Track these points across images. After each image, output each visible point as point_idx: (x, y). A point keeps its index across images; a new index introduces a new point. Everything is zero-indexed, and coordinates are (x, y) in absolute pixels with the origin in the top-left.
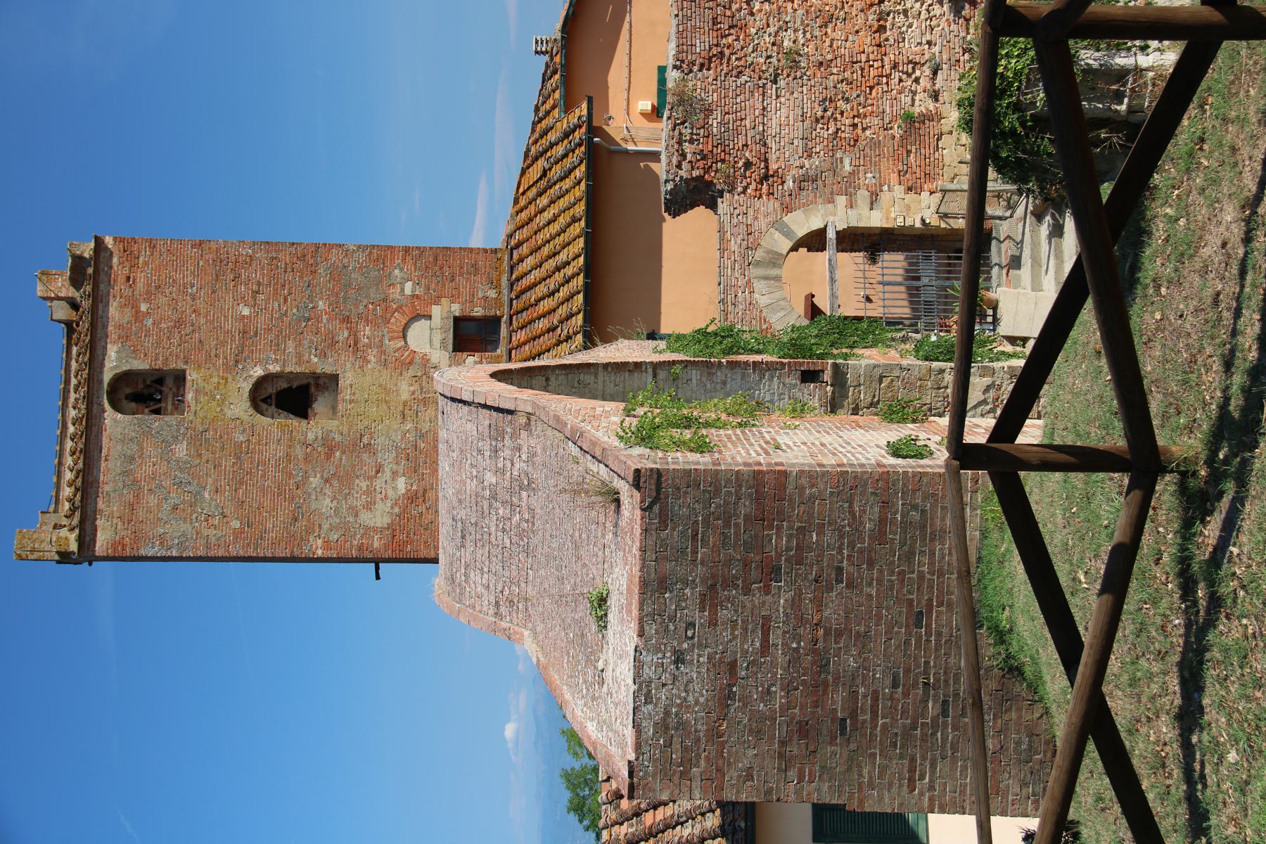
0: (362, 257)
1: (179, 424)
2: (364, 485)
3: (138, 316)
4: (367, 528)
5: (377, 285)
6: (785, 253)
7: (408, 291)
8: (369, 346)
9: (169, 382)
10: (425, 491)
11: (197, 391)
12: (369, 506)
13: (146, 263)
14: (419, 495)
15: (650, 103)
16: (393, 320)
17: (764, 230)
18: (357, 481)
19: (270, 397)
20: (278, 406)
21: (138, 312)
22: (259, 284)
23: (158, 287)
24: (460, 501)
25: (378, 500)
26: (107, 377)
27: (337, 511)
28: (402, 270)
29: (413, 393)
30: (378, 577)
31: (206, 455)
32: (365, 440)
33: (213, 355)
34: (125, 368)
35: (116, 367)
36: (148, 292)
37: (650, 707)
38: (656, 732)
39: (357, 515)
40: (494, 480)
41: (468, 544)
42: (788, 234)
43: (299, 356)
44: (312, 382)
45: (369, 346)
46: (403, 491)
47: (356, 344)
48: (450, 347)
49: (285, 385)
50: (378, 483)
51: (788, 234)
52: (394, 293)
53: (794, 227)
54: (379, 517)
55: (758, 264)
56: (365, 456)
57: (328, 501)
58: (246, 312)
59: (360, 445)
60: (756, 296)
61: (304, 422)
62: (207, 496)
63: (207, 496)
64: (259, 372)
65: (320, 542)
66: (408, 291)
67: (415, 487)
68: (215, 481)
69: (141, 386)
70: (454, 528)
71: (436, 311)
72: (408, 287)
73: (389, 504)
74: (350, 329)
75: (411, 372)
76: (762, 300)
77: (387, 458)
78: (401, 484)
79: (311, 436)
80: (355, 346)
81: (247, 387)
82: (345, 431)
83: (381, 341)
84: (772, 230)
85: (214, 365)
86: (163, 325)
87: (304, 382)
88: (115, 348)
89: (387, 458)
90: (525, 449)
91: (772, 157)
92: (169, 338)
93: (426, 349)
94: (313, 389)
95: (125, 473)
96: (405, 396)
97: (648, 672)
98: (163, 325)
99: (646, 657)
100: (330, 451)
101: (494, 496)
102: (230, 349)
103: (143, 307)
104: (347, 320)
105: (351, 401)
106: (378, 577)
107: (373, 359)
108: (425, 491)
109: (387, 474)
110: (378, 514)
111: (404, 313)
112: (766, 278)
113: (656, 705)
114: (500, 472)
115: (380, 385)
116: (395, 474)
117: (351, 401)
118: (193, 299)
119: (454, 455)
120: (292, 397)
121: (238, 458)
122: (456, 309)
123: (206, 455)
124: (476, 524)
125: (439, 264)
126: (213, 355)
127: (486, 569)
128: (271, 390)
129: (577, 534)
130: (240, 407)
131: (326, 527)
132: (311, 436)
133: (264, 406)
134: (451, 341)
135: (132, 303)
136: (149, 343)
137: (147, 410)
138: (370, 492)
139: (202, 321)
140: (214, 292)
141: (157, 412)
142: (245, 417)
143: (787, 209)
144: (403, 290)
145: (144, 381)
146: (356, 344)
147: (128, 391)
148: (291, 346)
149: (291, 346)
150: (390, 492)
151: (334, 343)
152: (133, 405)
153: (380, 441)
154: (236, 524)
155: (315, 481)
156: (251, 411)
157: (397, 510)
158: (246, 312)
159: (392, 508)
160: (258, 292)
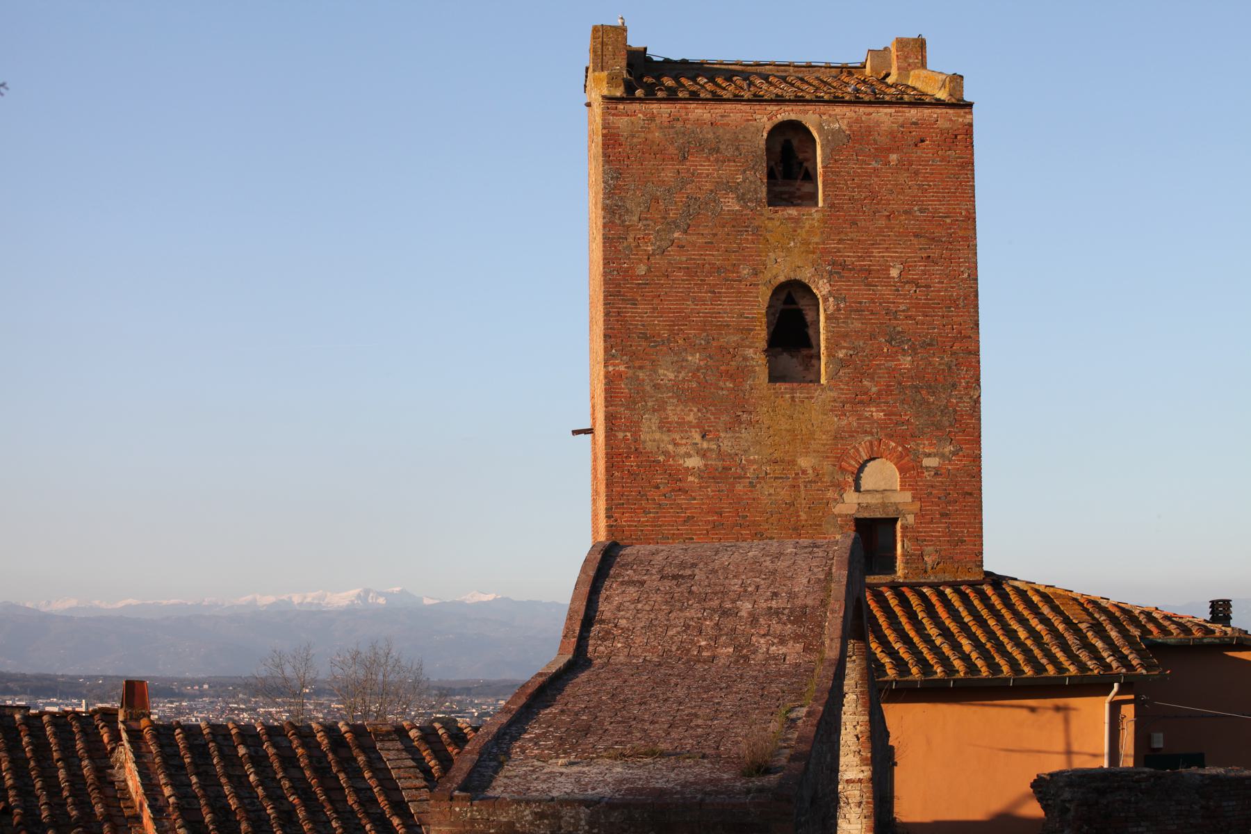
0: (965, 406)
1: (759, 202)
2: (691, 418)
5: (933, 424)
7: (927, 462)
9: (807, 188)
11: (796, 221)
12: (665, 426)
15: (1161, 746)
19: (794, 302)
20: (782, 311)
21: (890, 150)
24: (714, 571)
26: (810, 118)
27: (657, 387)
28: (955, 453)
30: (576, 432)
37: (529, 818)
38: (500, 824)
40: (743, 613)
41: (667, 583)
44: (814, 351)
47: (861, 402)
48: (861, 516)
49: (809, 318)
54: (651, 435)
56: (724, 418)
57: (672, 376)
58: (894, 273)
59: (738, 412)
61: (763, 345)
62: (676, 235)
63: (676, 235)
64: (821, 288)
65: (622, 368)
66: (927, 462)
68: (694, 244)
69: (801, 156)
70: (682, 565)
71: (907, 497)
73: (670, 448)
74: (879, 393)
75: (827, 466)
78: (694, 462)
80: (860, 400)
81: (805, 275)
82: (756, 393)
83: (866, 432)
85: (828, 238)
87: (814, 343)
88: (844, 127)
89: (726, 445)
90: (783, 650)
94: (805, 352)
95: (701, 145)
96: (803, 462)
97: (567, 813)
99: (584, 812)
100: (731, 377)
101: (725, 613)
102: (850, 257)
103: (894, 157)
104: (888, 390)
105: (793, 398)
106: (576, 432)
109: (705, 445)
110: (657, 436)
113: (532, 823)
114: (754, 619)
115: (813, 433)
116: (703, 454)
117: (793, 398)
118: (906, 212)
119: (768, 563)
120: (790, 327)
124: (690, 592)
125: (960, 497)
127: (640, 606)
128: (803, 303)
129: (700, 722)
130: (781, 271)
131: (641, 375)
132: (750, 352)
133: (783, 296)
134: (866, 515)
135: (896, 141)
137: (773, 163)
139: (882, 223)
140: (916, 236)
141: (771, 175)
144: (929, 455)
145: (807, 160)
146: (861, 402)
147: (795, 143)
149: (857, 325)
150: (682, 450)
152: (778, 148)
153: (746, 435)
155: (695, 359)
156: (776, 282)
157: (661, 458)
158: (894, 273)
159: (666, 453)
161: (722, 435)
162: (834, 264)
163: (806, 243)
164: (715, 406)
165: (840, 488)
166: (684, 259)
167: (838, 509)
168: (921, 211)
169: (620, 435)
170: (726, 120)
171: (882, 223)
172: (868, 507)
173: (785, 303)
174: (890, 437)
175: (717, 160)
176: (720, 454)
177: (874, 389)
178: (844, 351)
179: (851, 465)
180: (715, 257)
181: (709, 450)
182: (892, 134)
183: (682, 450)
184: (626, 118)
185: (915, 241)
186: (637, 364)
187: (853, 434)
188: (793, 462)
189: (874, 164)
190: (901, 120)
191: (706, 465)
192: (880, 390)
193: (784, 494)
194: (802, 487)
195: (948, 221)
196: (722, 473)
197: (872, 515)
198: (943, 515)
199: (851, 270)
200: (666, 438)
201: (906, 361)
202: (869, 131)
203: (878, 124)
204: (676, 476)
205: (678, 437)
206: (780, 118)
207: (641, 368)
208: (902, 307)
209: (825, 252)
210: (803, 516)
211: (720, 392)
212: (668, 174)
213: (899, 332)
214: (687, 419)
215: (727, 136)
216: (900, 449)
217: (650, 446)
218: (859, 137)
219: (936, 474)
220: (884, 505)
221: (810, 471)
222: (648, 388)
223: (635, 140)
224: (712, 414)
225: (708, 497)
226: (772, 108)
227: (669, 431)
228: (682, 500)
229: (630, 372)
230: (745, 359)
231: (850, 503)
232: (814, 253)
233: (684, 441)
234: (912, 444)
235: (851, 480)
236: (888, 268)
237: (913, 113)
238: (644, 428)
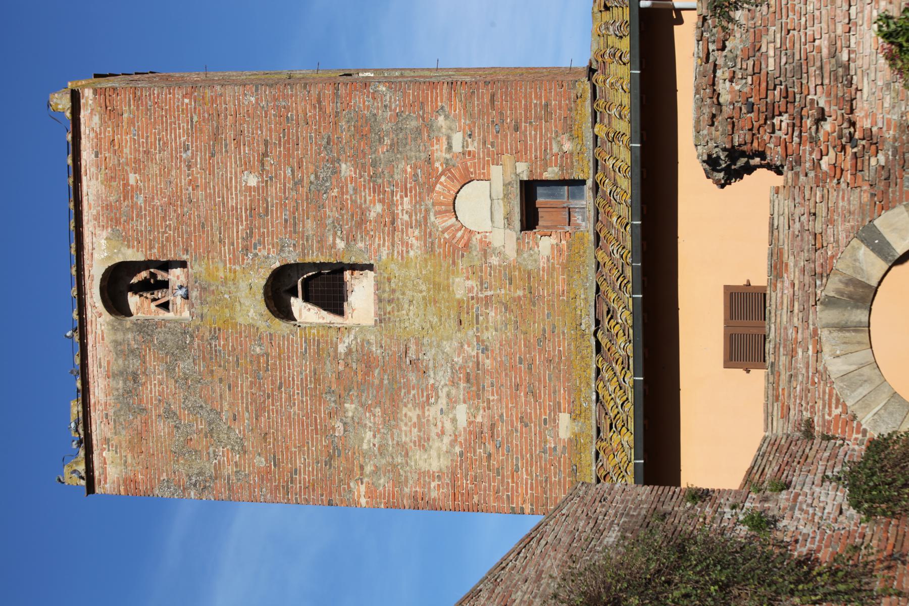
3: (127, 192)
4: (422, 474)
5: (415, 139)
6: (874, 283)
7: (457, 147)
8: (409, 225)
10: (493, 427)
12: (423, 443)
13: (131, 122)
14: (485, 430)
16: (438, 187)
17: (842, 237)
18: (405, 410)
20: (306, 299)
21: (126, 185)
22: (266, 143)
23: (147, 152)
25: (433, 435)
29: (470, 290)
31: (219, 372)
32: (412, 354)
33: (216, 240)
34: (117, 261)
35: (108, 258)
36: (137, 161)
39: (407, 454)
42: (881, 247)
43: (321, 241)
45: (409, 225)
46: (465, 424)
47: (393, 223)
48: (517, 224)
50: (432, 412)
51: (881, 247)
52: (440, 153)
53: (890, 237)
54: (435, 460)
55: (830, 302)
56: (413, 377)
57: (369, 435)
58: (253, 181)
60: (826, 356)
65: (363, 488)
66: (457, 147)
67: (479, 419)
68: (231, 405)
71: (496, 172)
72: (457, 140)
73: (447, 440)
74: (382, 201)
76: (836, 367)
77: (440, 378)
79: (342, 349)
80: (391, 223)
81: (260, 280)
83: (425, 218)
84: (855, 242)
86: (157, 202)
88: (105, 234)
91: (859, 114)
92: (164, 219)
93: (487, 226)
98: (157, 202)
103: (132, 178)
104: (377, 189)
105: (390, 301)
107: (414, 241)
108: (493, 427)
109: (443, 402)
110: (433, 453)
111: (452, 178)
112: (842, 327)
116: (452, 402)
118: (189, 167)
121: (257, 377)
122: (523, 171)
123: (219, 372)
126: (216, 240)
131: (368, 469)
132: (342, 349)
136: (142, 225)
138: (420, 425)
140: (213, 155)
142: (261, 324)
143: (884, 203)
144: (450, 148)
148: (310, 226)
149: (310, 226)
150: (448, 426)
151: (362, 222)
154: (260, 462)
157: (457, 449)
160: (265, 155)
161: (431, 381)
162: (246, 249)
163: (225, 282)
164: (400, 389)
165: (486, 249)
166: (247, 415)
167: (511, 253)
168: (186, 149)
169: (434, 494)
170: (104, 364)
171: (200, 193)
172: (508, 218)
173: (297, 296)
174: (431, 189)
175: (144, 373)
176: (454, 383)
177: (379, 208)
178: (338, 241)
179: (462, 237)
180: (244, 383)
181: (448, 395)
182: (108, 180)
183: (448, 426)
184: (108, 469)
185: (218, 157)
186: (357, 470)
187: (427, 235)
188: (460, 303)
189: (140, 201)
190: (93, 169)
191: (465, 402)
192: (380, 201)
193: (493, 315)
194: (489, 293)
195: (195, 119)
196: (472, 380)
197: (517, 209)
198: (517, 129)
199: (251, 232)
200: (436, 444)
201: (346, 169)
202: (108, 207)
203: (98, 196)
204: (477, 434)
205: (434, 431)
206: (99, 304)
207: (362, 468)
208: (289, 171)
209: (234, 260)
210: (520, 293)
211: (386, 382)
212: (162, 428)
213: (317, 177)
214: (415, 419)
215: (120, 362)
216: (443, 179)
217: (445, 463)
218: (113, 217)
219: (470, 136)
220: (506, 196)
221: (469, 283)
222: (384, 461)
223: (129, 460)
224: (409, 392)
225: (500, 400)
226: (90, 313)
227: (429, 439)
228: (502, 429)
229: (365, 480)
230: (349, 352)
231: (504, 238)
232: (235, 272)
233: (439, 424)
234: (437, 165)
235: (479, 236)
236: (249, 189)
237: (87, 156)
238: (424, 466)
